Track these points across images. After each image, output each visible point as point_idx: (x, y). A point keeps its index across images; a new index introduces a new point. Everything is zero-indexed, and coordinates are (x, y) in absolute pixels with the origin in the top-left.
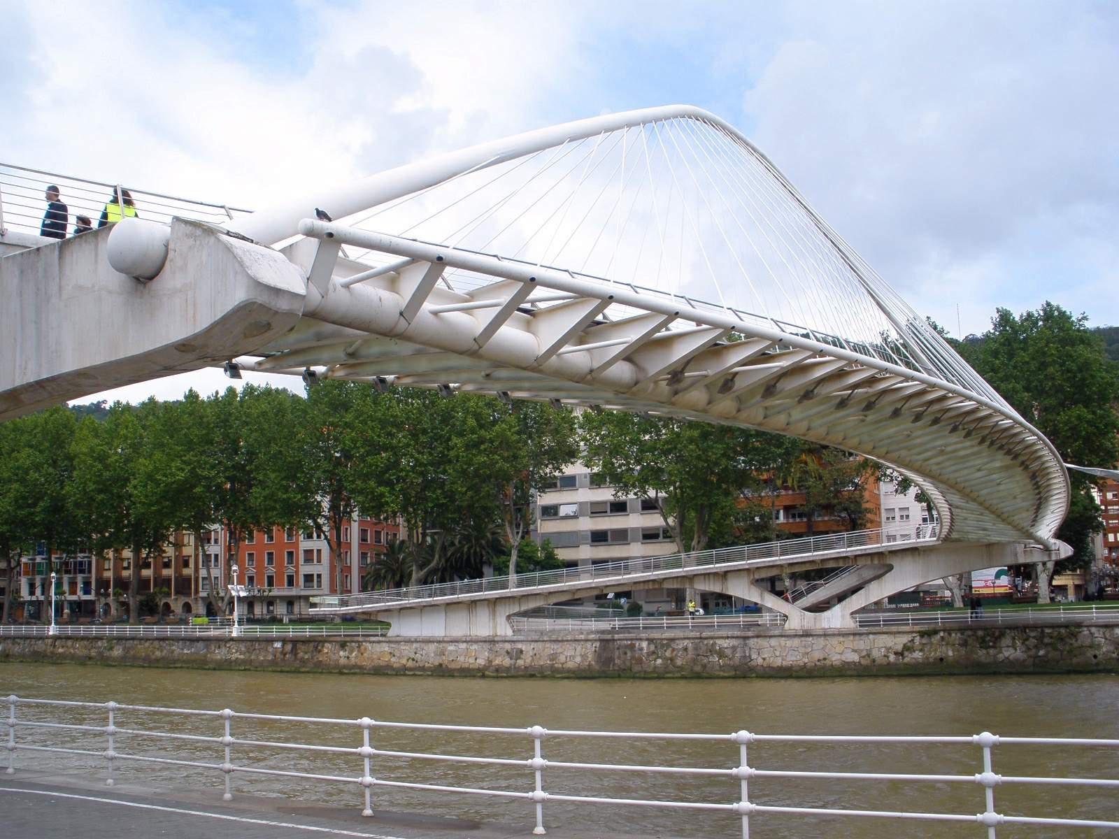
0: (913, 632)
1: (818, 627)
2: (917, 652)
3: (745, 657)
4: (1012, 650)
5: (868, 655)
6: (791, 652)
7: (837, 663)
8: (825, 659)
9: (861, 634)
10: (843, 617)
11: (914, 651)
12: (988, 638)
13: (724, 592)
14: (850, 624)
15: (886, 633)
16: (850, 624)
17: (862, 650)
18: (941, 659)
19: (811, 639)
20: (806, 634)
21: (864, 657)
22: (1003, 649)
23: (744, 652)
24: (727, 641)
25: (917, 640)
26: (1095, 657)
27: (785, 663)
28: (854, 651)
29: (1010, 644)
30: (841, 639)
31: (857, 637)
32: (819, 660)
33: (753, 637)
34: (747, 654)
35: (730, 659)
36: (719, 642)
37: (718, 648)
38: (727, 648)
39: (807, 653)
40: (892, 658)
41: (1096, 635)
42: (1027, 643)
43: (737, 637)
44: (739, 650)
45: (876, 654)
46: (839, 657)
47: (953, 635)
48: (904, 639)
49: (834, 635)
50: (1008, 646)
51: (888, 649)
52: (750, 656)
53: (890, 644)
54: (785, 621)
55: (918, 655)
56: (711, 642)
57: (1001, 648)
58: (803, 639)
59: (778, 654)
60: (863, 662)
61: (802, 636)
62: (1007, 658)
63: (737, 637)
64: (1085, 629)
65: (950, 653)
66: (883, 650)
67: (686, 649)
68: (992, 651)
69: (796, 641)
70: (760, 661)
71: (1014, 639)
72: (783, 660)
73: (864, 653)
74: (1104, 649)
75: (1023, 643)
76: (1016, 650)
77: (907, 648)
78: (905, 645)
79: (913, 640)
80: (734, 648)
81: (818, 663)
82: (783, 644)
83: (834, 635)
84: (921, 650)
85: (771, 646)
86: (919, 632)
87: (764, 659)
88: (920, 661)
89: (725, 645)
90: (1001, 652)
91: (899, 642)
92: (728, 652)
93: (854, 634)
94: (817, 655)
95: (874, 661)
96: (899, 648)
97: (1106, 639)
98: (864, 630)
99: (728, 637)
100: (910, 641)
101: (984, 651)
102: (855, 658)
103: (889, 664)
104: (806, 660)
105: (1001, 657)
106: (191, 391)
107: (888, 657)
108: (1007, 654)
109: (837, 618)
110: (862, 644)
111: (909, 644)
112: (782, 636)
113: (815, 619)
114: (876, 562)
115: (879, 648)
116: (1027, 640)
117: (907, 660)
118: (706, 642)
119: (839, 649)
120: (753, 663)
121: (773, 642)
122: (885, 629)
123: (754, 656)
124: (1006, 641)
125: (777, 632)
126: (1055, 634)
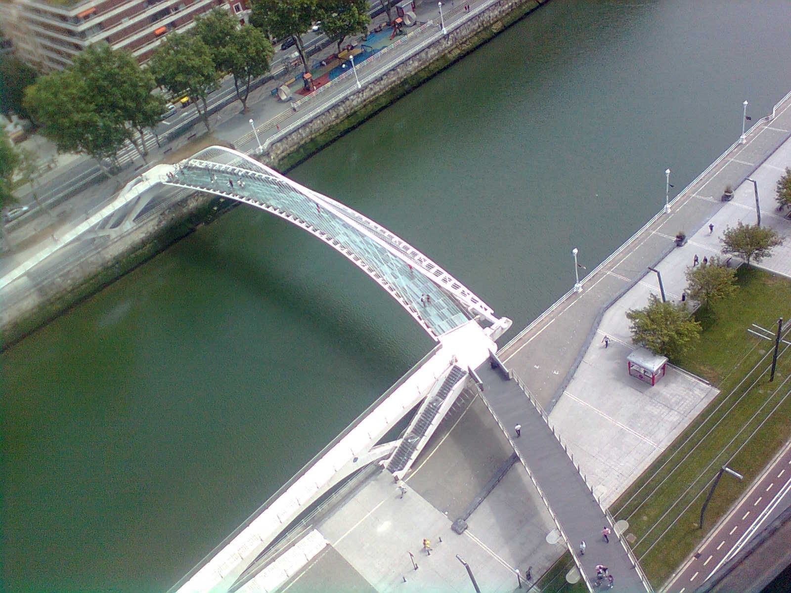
10: (130, 224)
25: (161, 217)
40: (156, 228)
55: (164, 222)
65: (174, 215)
67: (77, 271)
68: (186, 207)
70: (110, 257)
73: (146, 232)
77: (160, 222)
79: (159, 218)
90: (189, 206)
91: (155, 222)
94: (130, 243)
96: (157, 223)
102: (142, 236)
110: (144, 229)
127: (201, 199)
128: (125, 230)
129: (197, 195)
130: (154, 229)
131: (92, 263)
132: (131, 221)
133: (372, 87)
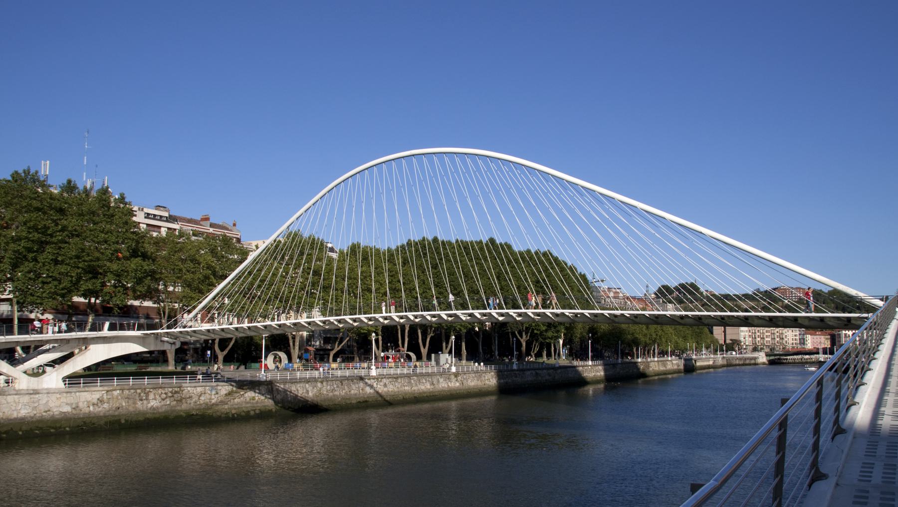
2: (106, 404)
4: (155, 402)
7: (57, 413)
8: (49, 411)
14: (61, 385)
15: (87, 391)
17: (72, 404)
21: (74, 408)
22: (151, 401)
27: (20, 415)
28: (67, 404)
30: (58, 396)
40: (91, 408)
49: (54, 393)
53: (90, 399)
55: (106, 406)
58: (32, 396)
64: (186, 388)
65: (124, 404)
66: (86, 403)
69: (26, 399)
73: (74, 406)
77: (101, 401)
81: (44, 414)
83: (54, 393)
85: (8, 403)
90: (149, 403)
100: (101, 397)
102: (67, 409)
104: (35, 412)
105: (149, 406)
106: (69, 182)
108: (152, 404)
109: (54, 379)
112: (16, 394)
119: (58, 403)
121: (10, 399)
126: (174, 391)
128: (45, 386)
133: (387, 383)
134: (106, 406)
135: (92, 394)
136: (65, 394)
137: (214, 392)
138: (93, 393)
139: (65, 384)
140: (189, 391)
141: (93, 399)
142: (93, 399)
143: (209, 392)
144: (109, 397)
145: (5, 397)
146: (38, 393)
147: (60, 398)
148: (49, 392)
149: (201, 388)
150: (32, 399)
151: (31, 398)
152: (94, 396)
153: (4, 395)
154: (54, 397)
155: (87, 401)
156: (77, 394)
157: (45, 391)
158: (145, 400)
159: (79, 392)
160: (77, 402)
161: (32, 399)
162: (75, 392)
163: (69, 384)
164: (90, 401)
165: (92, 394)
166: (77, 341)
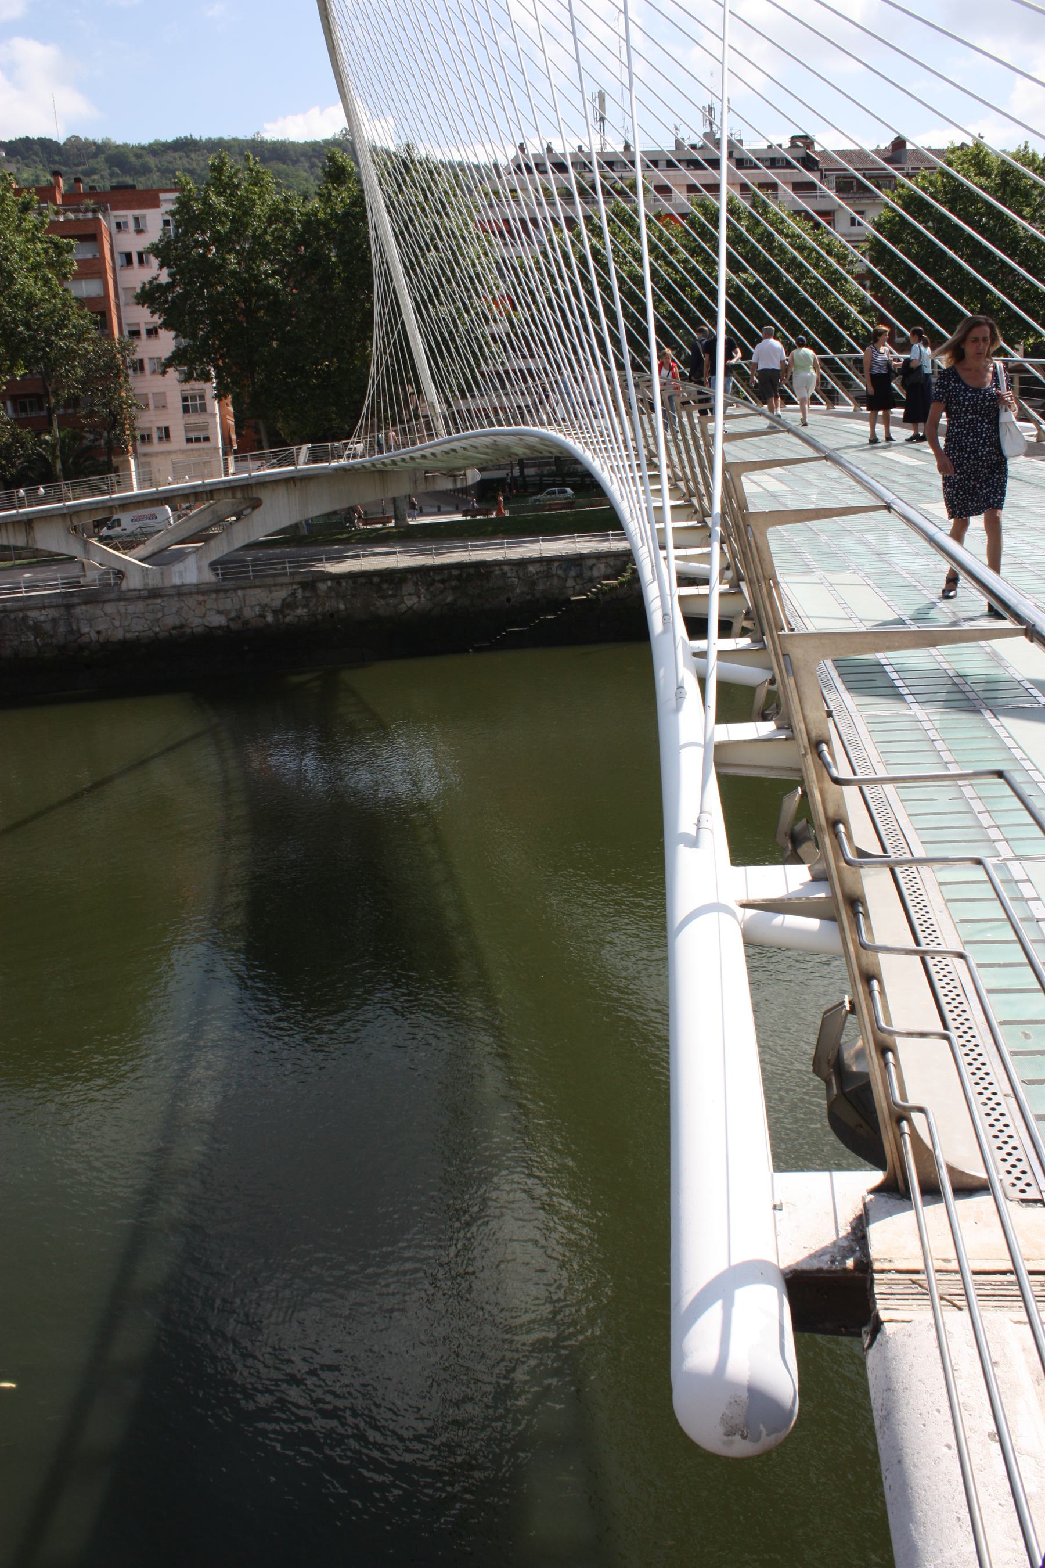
0: (292, 584)
1: (167, 583)
3: (71, 632)
5: (239, 617)
6: (135, 621)
7: (200, 629)
9: (226, 591)
11: (297, 607)
12: (385, 586)
13: (30, 545)
14: (209, 577)
15: (259, 587)
16: (209, 577)
17: (229, 611)
18: (332, 615)
19: (159, 601)
20: (154, 593)
21: (232, 619)
23: (70, 625)
24: (44, 612)
25: (300, 594)
26: (509, 600)
27: (128, 635)
28: (219, 612)
29: (412, 592)
30: (201, 598)
31: (221, 595)
32: (174, 628)
33: (79, 604)
34: (75, 627)
35: (51, 636)
36: (33, 614)
37: (31, 623)
38: (44, 622)
39: (158, 620)
40: (270, 618)
41: (509, 575)
42: (432, 589)
43: (58, 606)
44: (62, 623)
45: (248, 613)
46: (200, 621)
47: (344, 584)
48: (283, 594)
49: (191, 593)
50: (410, 594)
51: (264, 607)
52: (79, 630)
53: (266, 601)
54: (122, 579)
55: (300, 611)
56: (21, 615)
57: (402, 596)
58: (149, 601)
59: (117, 623)
60: (233, 625)
61: (148, 598)
62: (411, 608)
63: (58, 606)
65: (342, 606)
66: (257, 609)
68: (392, 601)
69: (140, 606)
70: (94, 636)
71: (416, 584)
72: (126, 631)
73: (233, 614)
74: (518, 591)
75: (427, 590)
76: (419, 597)
77: (287, 605)
78: (284, 600)
79: (293, 594)
80: (54, 621)
81: (174, 632)
82: (123, 610)
83: (191, 593)
84: (304, 606)
85: (106, 615)
86: (298, 583)
87: (99, 632)
88: (306, 618)
89: (42, 618)
91: (279, 595)
92: (47, 627)
93: (217, 591)
94: (171, 621)
95: (246, 623)
96: (277, 603)
97: (519, 578)
98: (230, 584)
99: (44, 608)
100: (290, 595)
101: (383, 602)
102: (217, 620)
103: (267, 625)
104: (157, 629)
105: (403, 607)
107: (264, 617)
108: (409, 603)
110: (230, 603)
111: (289, 600)
112: (119, 600)
113: (162, 574)
114: (239, 495)
115: (252, 607)
116: (432, 584)
117: (288, 619)
118: (12, 616)
120: (85, 639)
121: (110, 608)
122: (257, 582)
123: (85, 629)
124: (408, 588)
125: (113, 596)
127: (449, 599)
128: (177, 581)
129: (443, 581)
130: (262, 616)
131: (37, 628)
132: (205, 563)
134: (300, 611)
135: (271, 592)
136: (214, 596)
137: (573, 573)
138: (273, 588)
139: (217, 575)
140: (504, 574)
141: (272, 600)
142: (272, 600)
143: (560, 572)
144: (308, 594)
145: (101, 605)
146: (161, 596)
147: (205, 601)
148: (180, 592)
149: (537, 565)
150: (151, 607)
151: (148, 605)
152: (274, 595)
153: (98, 602)
154: (191, 601)
155: (260, 605)
156: (240, 592)
157: (173, 591)
158: (392, 596)
159: (243, 588)
160: (238, 607)
161: (151, 607)
162: (235, 590)
163: (223, 574)
164: (266, 605)
165: (271, 592)
166: (230, 494)
